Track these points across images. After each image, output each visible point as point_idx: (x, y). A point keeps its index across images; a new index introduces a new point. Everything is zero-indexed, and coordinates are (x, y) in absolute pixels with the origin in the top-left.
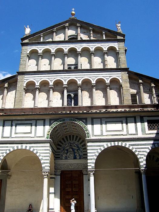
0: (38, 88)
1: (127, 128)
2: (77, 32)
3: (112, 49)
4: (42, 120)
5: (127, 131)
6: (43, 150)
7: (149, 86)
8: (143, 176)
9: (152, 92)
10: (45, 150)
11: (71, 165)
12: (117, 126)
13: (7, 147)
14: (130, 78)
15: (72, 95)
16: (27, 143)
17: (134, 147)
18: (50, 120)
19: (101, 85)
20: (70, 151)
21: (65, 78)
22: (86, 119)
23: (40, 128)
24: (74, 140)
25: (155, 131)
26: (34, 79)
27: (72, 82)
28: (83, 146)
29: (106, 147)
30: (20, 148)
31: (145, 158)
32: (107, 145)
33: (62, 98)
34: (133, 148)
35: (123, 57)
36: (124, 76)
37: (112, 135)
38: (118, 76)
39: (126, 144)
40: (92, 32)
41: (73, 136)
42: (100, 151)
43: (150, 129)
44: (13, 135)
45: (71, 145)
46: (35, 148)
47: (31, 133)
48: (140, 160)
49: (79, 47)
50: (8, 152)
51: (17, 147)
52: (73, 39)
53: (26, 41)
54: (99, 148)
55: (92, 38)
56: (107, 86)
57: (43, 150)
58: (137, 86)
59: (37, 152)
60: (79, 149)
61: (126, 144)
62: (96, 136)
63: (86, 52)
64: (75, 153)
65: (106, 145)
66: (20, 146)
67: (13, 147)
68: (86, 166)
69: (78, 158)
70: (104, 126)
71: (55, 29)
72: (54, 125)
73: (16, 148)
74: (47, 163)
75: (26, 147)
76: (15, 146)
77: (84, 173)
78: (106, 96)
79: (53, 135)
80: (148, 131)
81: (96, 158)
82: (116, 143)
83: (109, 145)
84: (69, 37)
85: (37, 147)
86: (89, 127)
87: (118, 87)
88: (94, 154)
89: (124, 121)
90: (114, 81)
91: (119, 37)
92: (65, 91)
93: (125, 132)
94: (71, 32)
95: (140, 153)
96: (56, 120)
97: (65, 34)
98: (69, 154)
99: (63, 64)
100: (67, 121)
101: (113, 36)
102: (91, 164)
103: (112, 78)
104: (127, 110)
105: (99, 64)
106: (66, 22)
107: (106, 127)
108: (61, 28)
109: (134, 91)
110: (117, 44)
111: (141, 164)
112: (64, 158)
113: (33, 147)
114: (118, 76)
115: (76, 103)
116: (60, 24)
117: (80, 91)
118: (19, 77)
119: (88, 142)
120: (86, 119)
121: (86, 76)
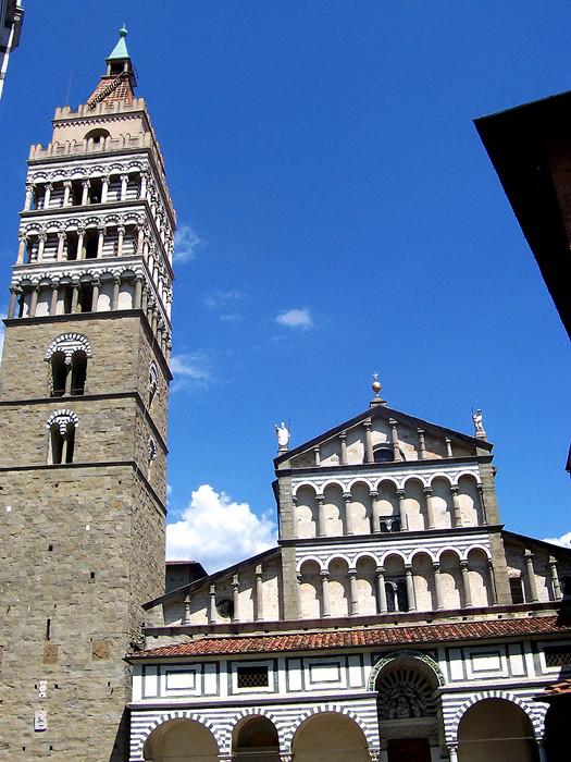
0: (326, 575)
1: (509, 664)
2: (390, 437)
3: (467, 479)
4: (356, 654)
5: (510, 670)
6: (365, 712)
7: (546, 559)
8: (541, 752)
9: (552, 575)
10: (370, 711)
11: (406, 728)
12: (491, 662)
13: (300, 709)
14: (505, 544)
15: (394, 585)
16: (335, 701)
17: (524, 699)
18: (372, 654)
19: (451, 563)
20: (402, 703)
21: (379, 552)
22: (435, 650)
23: (355, 671)
24: (407, 679)
25: (558, 669)
26: (316, 555)
27: (394, 560)
28: (424, 691)
29: (475, 701)
30: (323, 709)
31: (543, 719)
32: (476, 697)
33: (376, 592)
34: (521, 702)
35: (488, 498)
36: (494, 544)
37: (484, 679)
38: (482, 544)
39: (508, 695)
40: (422, 439)
41: (405, 672)
42: (464, 710)
43: (549, 664)
44: (308, 687)
45: (402, 691)
46: (351, 709)
47: (339, 680)
48: (534, 723)
49: (400, 478)
50: (303, 718)
51: (319, 708)
52: (384, 457)
53: (285, 466)
54: (462, 703)
55: (427, 456)
56: (462, 567)
57: (365, 712)
58: (520, 561)
59: (356, 716)
60: (418, 697)
61: (508, 695)
62: (455, 681)
63: (416, 490)
64: (411, 705)
65: (474, 697)
66: (323, 706)
67: (312, 709)
68: (438, 730)
69: (418, 715)
70: (468, 661)
71: (344, 432)
72: (382, 663)
73: (316, 711)
74: (375, 735)
75: (335, 707)
76: (315, 706)
77: (431, 743)
78: (461, 586)
79: (383, 683)
80: (545, 670)
81: (458, 721)
82: (492, 694)
83: (480, 698)
84: (374, 447)
85: (355, 706)
86: (442, 665)
87: (484, 564)
88: (454, 715)
89: (503, 651)
90: (476, 554)
91: (481, 452)
92: (382, 582)
93: (505, 673)
94: (377, 437)
95: (534, 711)
96: (383, 655)
97: (365, 442)
98: (399, 708)
99: (370, 516)
100: (403, 656)
101: (468, 448)
102: (451, 732)
103: (471, 547)
104: (505, 616)
105: (444, 513)
106: (366, 415)
107: (472, 663)
108: (356, 428)
109: (516, 572)
110: (477, 467)
111: (537, 730)
112: (391, 716)
113: (347, 707)
114: (482, 544)
115: (404, 605)
116: (353, 422)
117: (409, 578)
118: (285, 552)
119: (443, 693)
120: (435, 650)
121: (422, 546)
